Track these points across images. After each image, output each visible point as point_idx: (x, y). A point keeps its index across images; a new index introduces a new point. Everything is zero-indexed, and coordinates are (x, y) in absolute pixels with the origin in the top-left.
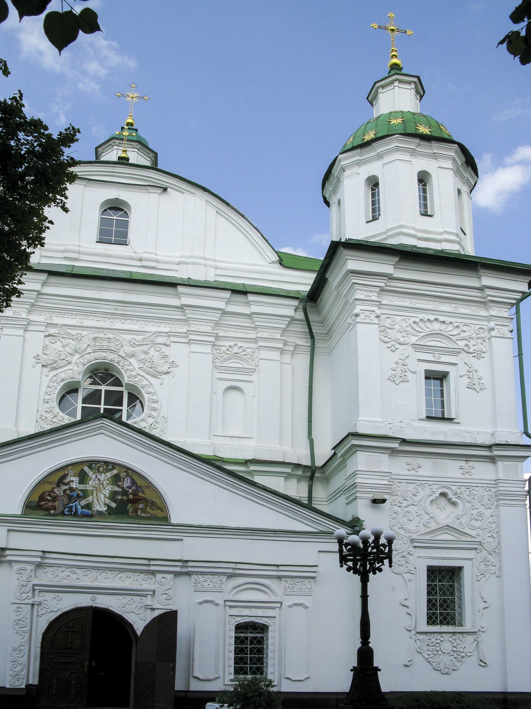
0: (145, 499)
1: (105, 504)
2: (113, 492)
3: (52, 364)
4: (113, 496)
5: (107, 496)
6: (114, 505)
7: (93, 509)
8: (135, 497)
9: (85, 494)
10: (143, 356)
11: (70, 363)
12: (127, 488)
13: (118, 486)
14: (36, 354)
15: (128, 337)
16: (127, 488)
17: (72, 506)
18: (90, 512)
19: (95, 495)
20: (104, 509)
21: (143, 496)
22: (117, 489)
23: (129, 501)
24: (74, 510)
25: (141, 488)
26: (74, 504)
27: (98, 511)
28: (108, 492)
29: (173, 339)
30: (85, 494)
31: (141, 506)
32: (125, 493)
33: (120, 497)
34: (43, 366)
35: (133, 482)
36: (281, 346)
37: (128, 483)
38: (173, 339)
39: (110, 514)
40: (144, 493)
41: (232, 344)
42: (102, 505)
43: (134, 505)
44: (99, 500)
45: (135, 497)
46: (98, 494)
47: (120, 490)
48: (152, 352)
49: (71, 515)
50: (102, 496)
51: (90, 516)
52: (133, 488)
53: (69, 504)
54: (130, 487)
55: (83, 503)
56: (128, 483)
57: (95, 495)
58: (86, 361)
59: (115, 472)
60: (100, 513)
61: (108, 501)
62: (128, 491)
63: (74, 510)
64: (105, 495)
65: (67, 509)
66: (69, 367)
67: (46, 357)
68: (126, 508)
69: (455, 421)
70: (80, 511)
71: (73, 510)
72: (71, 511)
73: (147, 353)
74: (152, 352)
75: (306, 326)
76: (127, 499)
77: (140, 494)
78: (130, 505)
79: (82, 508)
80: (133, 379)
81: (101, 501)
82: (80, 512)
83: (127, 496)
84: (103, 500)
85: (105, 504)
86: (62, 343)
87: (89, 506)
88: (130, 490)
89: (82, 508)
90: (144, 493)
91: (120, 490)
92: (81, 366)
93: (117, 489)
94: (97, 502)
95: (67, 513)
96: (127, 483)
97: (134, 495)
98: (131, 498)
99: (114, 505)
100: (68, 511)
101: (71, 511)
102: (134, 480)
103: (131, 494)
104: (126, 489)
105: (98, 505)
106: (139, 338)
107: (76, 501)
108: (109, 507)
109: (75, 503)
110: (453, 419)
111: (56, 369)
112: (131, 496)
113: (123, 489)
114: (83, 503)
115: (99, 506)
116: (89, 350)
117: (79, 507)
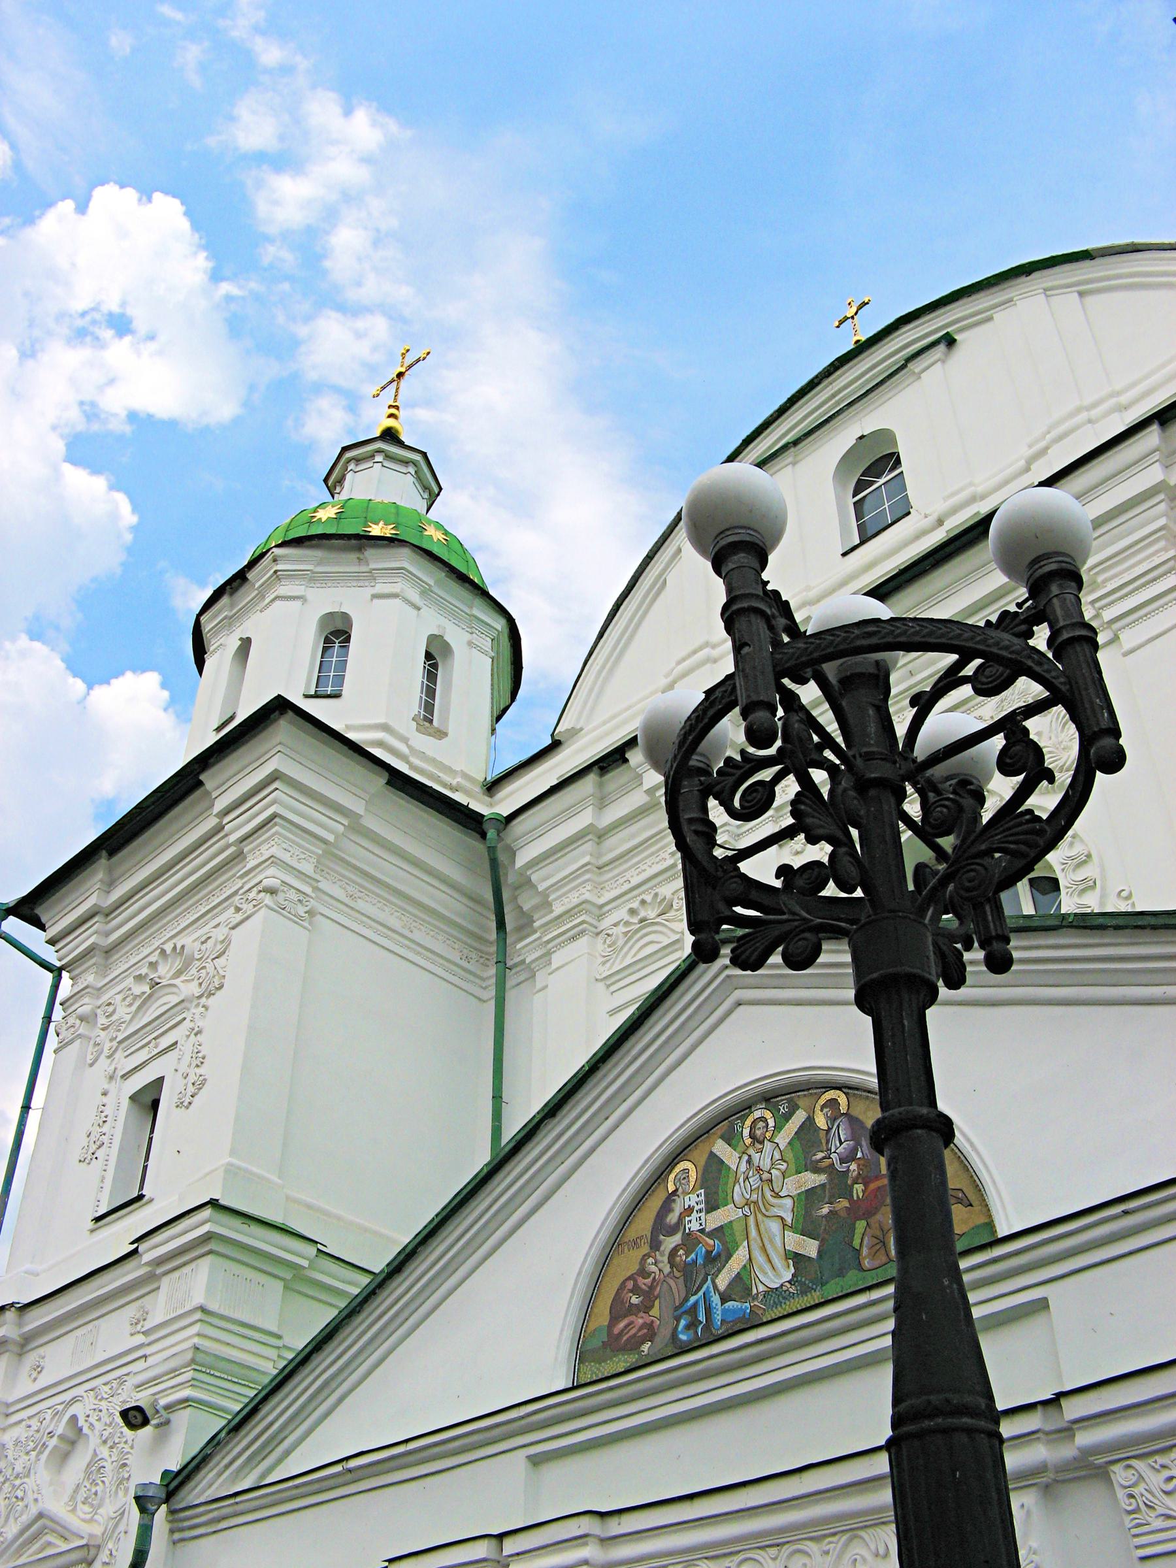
2: (803, 1197)
5: (789, 1220)
6: (811, 1248)
7: (754, 1291)
8: (872, 1186)
12: (842, 1161)
13: (816, 1170)
16: (842, 1161)
20: (782, 1275)
22: (812, 1180)
24: (702, 1317)
26: (701, 1293)
27: (770, 1291)
28: (788, 1202)
33: (825, 1210)
37: (841, 1143)
43: (872, 1221)
44: (768, 1246)
45: (872, 1186)
46: (762, 1227)
47: (822, 1178)
50: (775, 1227)
52: (859, 1155)
53: (686, 1300)
56: (841, 1143)
57: (753, 1233)
61: (795, 1242)
62: (848, 1170)
63: (702, 1317)
64: (782, 1218)
65: (683, 1323)
68: (850, 1245)
70: (719, 1312)
71: (700, 1319)
72: (692, 1325)
76: (848, 1205)
79: (724, 1299)
81: (775, 1249)
82: (719, 1317)
83: (847, 1193)
84: (778, 1240)
87: (741, 1285)
88: (853, 1166)
89: (724, 1299)
91: (822, 1178)
93: (812, 1180)
95: (683, 1337)
98: (861, 1195)
99: (811, 1248)
102: (857, 1120)
104: (837, 1166)
105: (767, 1267)
107: (705, 1280)
108: (797, 1258)
109: (705, 1286)
112: (859, 1188)
113: (830, 1175)
115: (770, 1272)
117: (716, 1299)
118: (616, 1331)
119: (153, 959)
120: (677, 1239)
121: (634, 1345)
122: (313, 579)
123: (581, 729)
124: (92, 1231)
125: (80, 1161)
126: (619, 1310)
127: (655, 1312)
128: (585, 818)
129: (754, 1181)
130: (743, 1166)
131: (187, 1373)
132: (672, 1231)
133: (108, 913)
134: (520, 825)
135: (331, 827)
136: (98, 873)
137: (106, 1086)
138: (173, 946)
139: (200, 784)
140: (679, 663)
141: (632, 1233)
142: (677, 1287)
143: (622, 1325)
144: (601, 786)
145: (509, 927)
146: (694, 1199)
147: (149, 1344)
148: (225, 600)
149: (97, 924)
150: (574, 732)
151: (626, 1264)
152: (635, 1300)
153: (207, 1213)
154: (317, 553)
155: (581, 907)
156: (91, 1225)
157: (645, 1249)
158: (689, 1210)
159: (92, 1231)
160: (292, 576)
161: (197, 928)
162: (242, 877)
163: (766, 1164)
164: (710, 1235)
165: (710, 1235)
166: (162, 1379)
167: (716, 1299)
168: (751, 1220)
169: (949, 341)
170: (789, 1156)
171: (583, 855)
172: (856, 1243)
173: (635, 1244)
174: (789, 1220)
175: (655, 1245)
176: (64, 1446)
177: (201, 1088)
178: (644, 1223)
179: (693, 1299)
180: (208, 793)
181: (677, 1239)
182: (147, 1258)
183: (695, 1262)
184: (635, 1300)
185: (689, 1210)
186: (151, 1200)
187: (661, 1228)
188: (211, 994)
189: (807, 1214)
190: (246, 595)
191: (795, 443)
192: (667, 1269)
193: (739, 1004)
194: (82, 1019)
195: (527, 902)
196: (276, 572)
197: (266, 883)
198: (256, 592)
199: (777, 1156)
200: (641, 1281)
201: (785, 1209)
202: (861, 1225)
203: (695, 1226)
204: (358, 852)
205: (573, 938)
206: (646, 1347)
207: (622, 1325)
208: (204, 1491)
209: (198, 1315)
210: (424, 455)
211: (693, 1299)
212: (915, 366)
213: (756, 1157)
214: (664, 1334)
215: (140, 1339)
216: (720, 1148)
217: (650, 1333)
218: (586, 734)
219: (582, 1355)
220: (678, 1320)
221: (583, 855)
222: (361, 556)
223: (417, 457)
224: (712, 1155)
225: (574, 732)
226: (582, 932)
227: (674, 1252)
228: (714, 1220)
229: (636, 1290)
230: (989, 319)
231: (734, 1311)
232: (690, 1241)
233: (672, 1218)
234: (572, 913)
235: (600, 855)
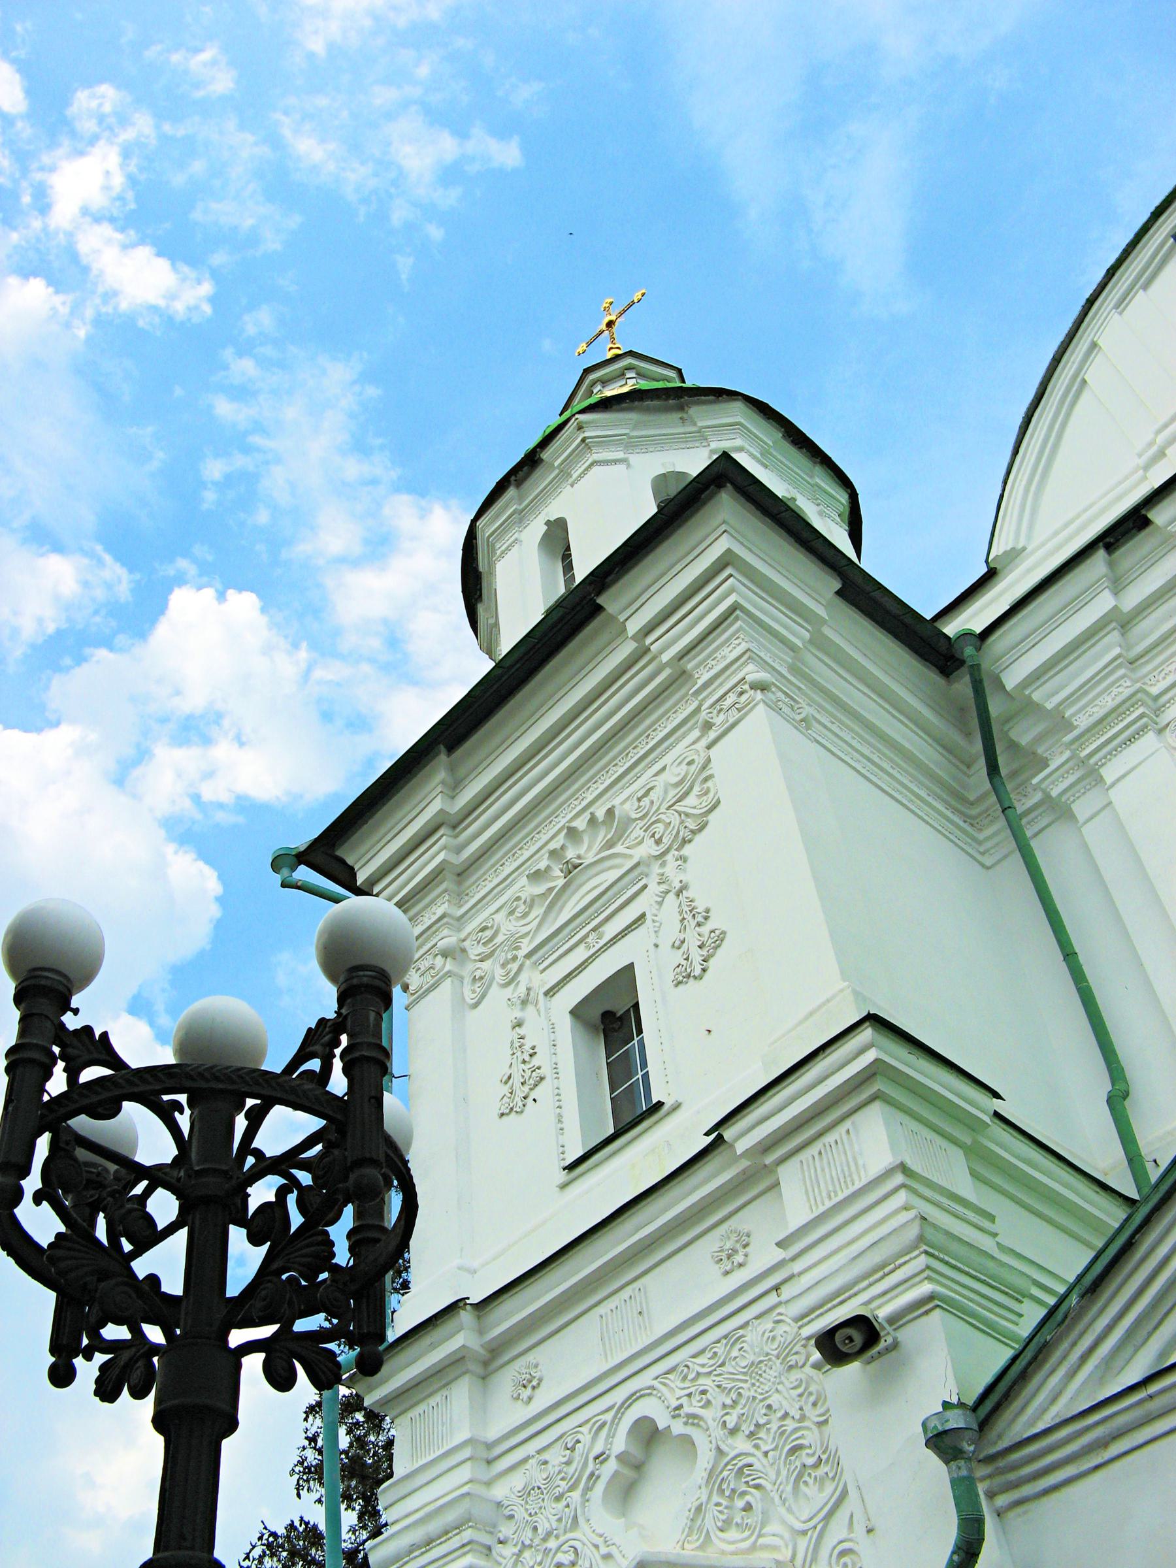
119: (555, 845)
122: (631, 444)
123: (1024, 549)
124: (563, 1186)
125: (502, 1115)
128: (1104, 603)
131: (913, 1262)
133: (456, 823)
135: (799, 635)
136: (438, 773)
137: (519, 1014)
138: (589, 816)
139: (599, 609)
140: (1159, 432)
144: (1111, 565)
145: (1004, 771)
147: (794, 1259)
148: (511, 492)
149: (444, 838)
150: (1014, 555)
154: (633, 416)
155: (1134, 699)
156: (563, 1176)
159: (563, 1186)
160: (604, 442)
161: (622, 788)
162: (698, 692)
166: (856, 1289)
171: (1110, 647)
176: (627, 1472)
177: (719, 946)
180: (613, 618)
182: (741, 1147)
186: (676, 1107)
188: (685, 842)
190: (539, 481)
194: (445, 954)
195: (1024, 734)
196: (583, 440)
197: (749, 678)
198: (557, 471)
208: (1044, 1410)
209: (899, 1179)
218: (1032, 553)
221: (1109, 648)
222: (685, 416)
225: (1014, 555)
226: (1144, 728)
234: (1121, 710)
235: (1129, 648)
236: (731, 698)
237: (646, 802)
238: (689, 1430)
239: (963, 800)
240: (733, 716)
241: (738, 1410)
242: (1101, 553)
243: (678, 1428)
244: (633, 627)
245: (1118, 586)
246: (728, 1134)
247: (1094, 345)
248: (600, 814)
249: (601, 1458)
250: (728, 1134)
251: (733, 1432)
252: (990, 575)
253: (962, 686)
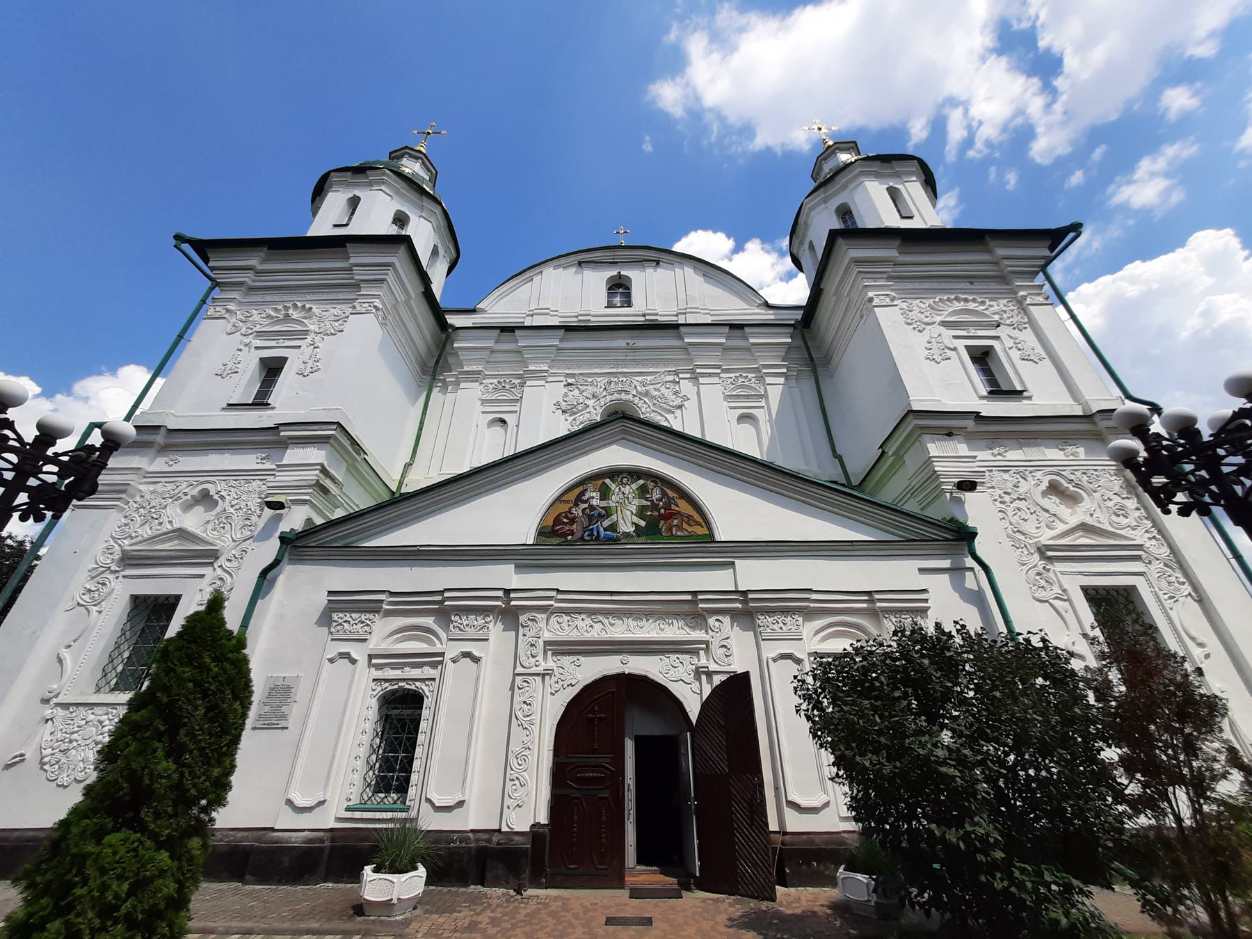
0: (679, 512)
1: (633, 523)
3: (571, 409)
4: (641, 512)
5: (634, 512)
6: (643, 523)
9: (608, 512)
10: (656, 393)
11: (588, 406)
14: (555, 402)
15: (640, 379)
17: (593, 529)
18: (615, 535)
19: (619, 512)
21: (677, 509)
22: (644, 503)
23: (661, 517)
24: (595, 533)
25: (673, 499)
27: (624, 533)
28: (635, 507)
29: (681, 376)
30: (608, 512)
31: (675, 522)
32: (654, 507)
33: (649, 513)
34: (563, 411)
35: (664, 494)
36: (785, 370)
38: (681, 376)
39: (639, 536)
40: (677, 506)
41: (738, 375)
42: (629, 525)
47: (649, 503)
48: (663, 389)
49: (592, 540)
50: (629, 513)
51: (615, 541)
53: (589, 526)
54: (660, 500)
55: (606, 523)
57: (619, 512)
58: (603, 403)
59: (641, 482)
60: (627, 535)
61: (636, 519)
63: (595, 533)
65: (586, 533)
66: (588, 410)
67: (564, 403)
69: (1025, 394)
72: (591, 535)
73: (658, 390)
74: (663, 389)
75: (806, 353)
77: (673, 507)
78: (662, 522)
79: (605, 530)
80: (648, 415)
84: (629, 517)
85: (633, 523)
86: (579, 389)
87: (613, 527)
90: (677, 506)
91: (649, 503)
92: (598, 408)
93: (644, 503)
94: (622, 522)
96: (656, 495)
97: (665, 509)
99: (643, 523)
100: (588, 535)
101: (591, 535)
103: (662, 508)
106: (649, 378)
107: (597, 522)
108: (637, 525)
110: (1021, 392)
111: (576, 413)
112: (662, 511)
114: (606, 523)
116: (605, 393)
117: (602, 529)
118: (556, 529)
120: (586, 505)
121: (564, 535)
124: (223, 409)
126: (557, 521)
127: (575, 526)
128: (490, 344)
129: (621, 496)
130: (617, 490)
132: (585, 502)
133: (258, 272)
134: (461, 333)
135: (401, 297)
137: (242, 348)
141: (565, 498)
142: (586, 523)
143: (558, 527)
144: (499, 335)
146: (596, 495)
147: (278, 471)
148: (349, 174)
149: (251, 274)
151: (564, 508)
152: (565, 520)
153: (334, 427)
154: (404, 185)
157: (572, 505)
158: (593, 498)
159: (223, 409)
160: (389, 185)
163: (627, 492)
164: (601, 508)
165: (601, 508)
167: (602, 529)
168: (619, 508)
169: (658, 263)
170: (637, 492)
172: (660, 527)
173: (567, 502)
174: (634, 512)
175: (576, 505)
176: (192, 502)
178: (572, 496)
179: (591, 527)
180: (348, 253)
181: (586, 505)
183: (593, 515)
184: (565, 520)
185: (593, 498)
186: (274, 408)
187: (579, 500)
188: (327, 334)
189: (642, 512)
190: (360, 179)
191: (596, 263)
192: (581, 514)
193: (623, 439)
195: (451, 360)
197: (375, 304)
199: (631, 491)
200: (569, 515)
201: (634, 509)
202: (662, 522)
203: (595, 503)
204: (403, 310)
205: (473, 381)
206: (569, 538)
207: (558, 527)
210: (437, 172)
211: (591, 527)
212: (646, 264)
213: (623, 489)
214: (578, 535)
215: (275, 467)
216: (607, 481)
217: (572, 533)
219: (542, 533)
220: (585, 532)
223: (434, 172)
224: (604, 482)
225: (483, 311)
226: (477, 381)
227: (584, 510)
228: (604, 504)
229: (566, 517)
230: (673, 264)
231: (609, 535)
232: (592, 508)
233: (585, 498)
236: (366, 305)
237: (324, 313)
238: (219, 499)
239: (425, 364)
240: (363, 310)
241: (236, 501)
242: (498, 331)
243: (216, 497)
244: (352, 260)
245: (497, 342)
246: (281, 428)
247: (542, 272)
248: (308, 306)
249: (186, 494)
250: (281, 428)
251: (232, 506)
252: (473, 311)
253: (444, 336)
